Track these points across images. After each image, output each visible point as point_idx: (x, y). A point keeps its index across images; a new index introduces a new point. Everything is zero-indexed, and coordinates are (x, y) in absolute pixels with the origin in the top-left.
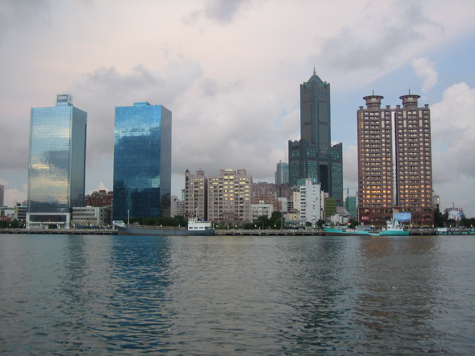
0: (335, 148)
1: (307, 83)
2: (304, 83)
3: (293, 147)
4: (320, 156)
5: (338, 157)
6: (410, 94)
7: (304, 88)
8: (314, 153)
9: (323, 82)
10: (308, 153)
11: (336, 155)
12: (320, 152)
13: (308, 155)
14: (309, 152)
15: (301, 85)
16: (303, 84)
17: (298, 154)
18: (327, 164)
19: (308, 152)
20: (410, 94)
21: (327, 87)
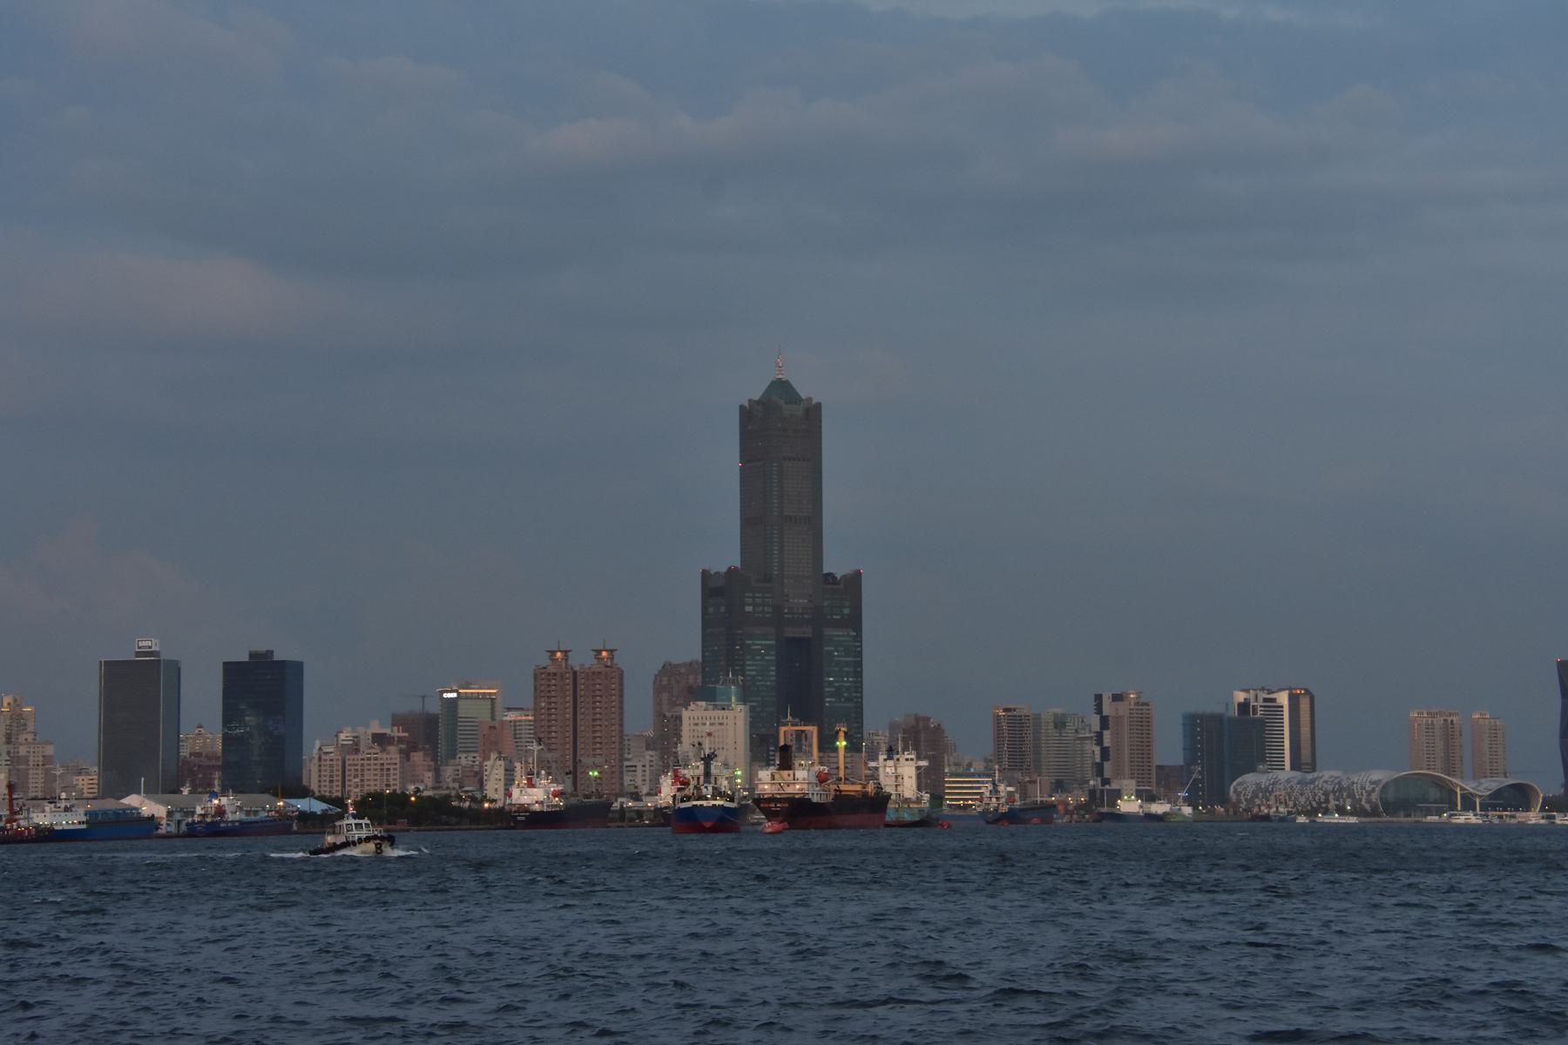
0: (835, 587)
1: (758, 402)
2: (750, 401)
3: (716, 590)
4: (787, 613)
5: (846, 611)
6: (604, 647)
7: (746, 414)
9: (804, 396)
10: (749, 609)
12: (787, 601)
13: (749, 612)
14: (754, 605)
15: (742, 407)
16: (746, 404)
17: (722, 609)
18: (810, 635)
19: (750, 605)
20: (604, 647)
21: (813, 413)
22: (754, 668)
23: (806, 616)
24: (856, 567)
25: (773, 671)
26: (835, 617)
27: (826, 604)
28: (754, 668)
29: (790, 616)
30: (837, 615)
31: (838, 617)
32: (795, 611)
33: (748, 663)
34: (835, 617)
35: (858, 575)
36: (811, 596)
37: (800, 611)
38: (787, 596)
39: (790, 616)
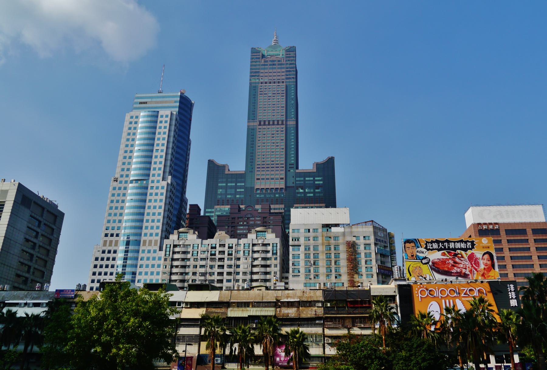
24: (330, 156)
29: (262, 196)
35: (330, 162)
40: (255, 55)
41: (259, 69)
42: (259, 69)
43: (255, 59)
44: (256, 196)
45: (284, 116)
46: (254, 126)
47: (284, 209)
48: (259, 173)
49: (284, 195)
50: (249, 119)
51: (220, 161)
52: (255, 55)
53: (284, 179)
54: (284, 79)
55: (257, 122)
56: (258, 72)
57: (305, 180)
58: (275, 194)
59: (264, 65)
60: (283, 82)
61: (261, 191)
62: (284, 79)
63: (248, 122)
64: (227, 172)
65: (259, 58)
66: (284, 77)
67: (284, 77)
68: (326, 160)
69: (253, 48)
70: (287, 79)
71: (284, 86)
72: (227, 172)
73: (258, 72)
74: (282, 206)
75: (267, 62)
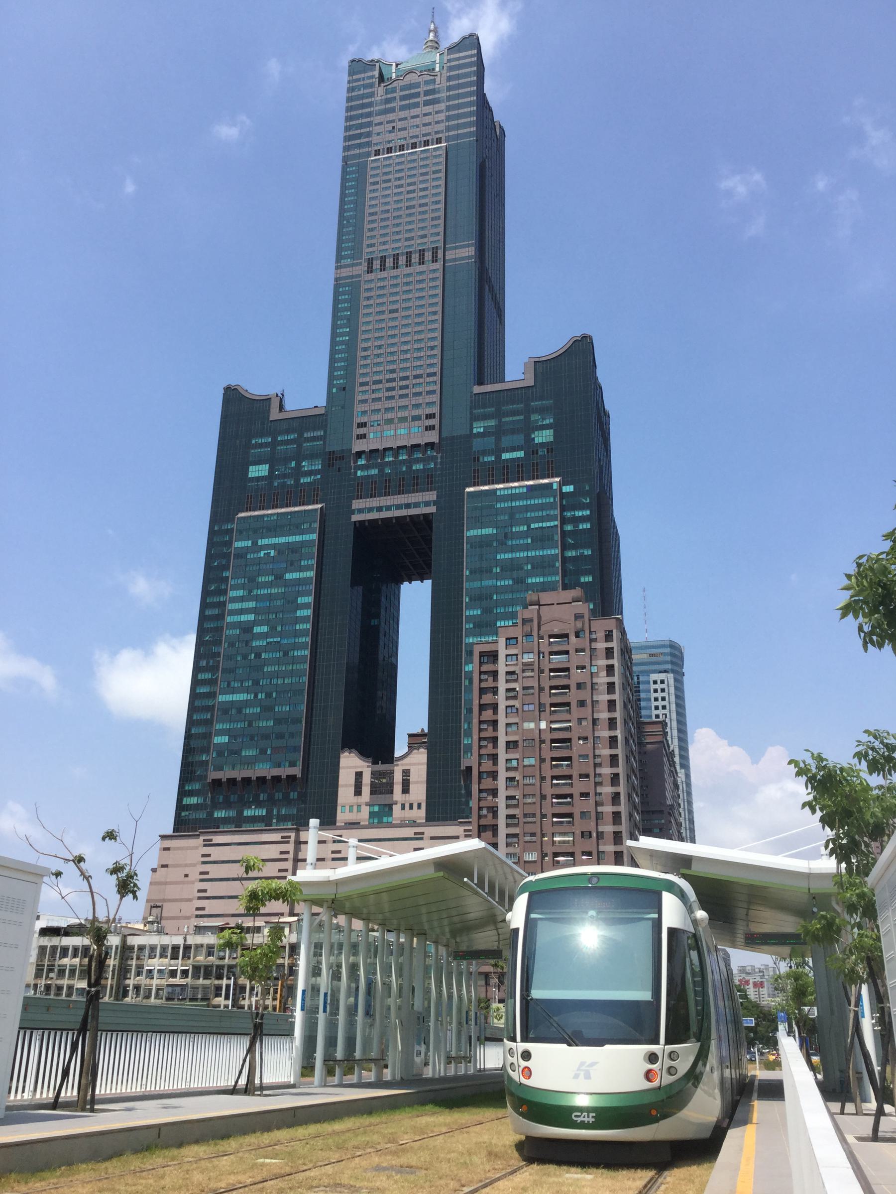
5: (543, 437)
8: (311, 457)
10: (258, 471)
11: (529, 428)
13: (258, 479)
14: (272, 461)
18: (432, 509)
22: (252, 604)
23: (420, 466)
25: (305, 606)
26: (505, 456)
27: (479, 428)
28: (252, 604)
29: (374, 472)
30: (513, 449)
31: (520, 454)
32: (390, 459)
33: (233, 594)
34: (505, 456)
36: (430, 416)
37: (403, 457)
38: (362, 425)
39: (374, 472)
40: (358, 80)
41: (369, 115)
42: (369, 115)
43: (359, 90)
44: (356, 473)
45: (441, 237)
46: (352, 277)
47: (435, 503)
48: (364, 407)
49: (435, 464)
50: (339, 257)
51: (256, 388)
52: (358, 80)
53: (437, 416)
54: (442, 132)
55: (361, 264)
56: (369, 124)
57: (498, 415)
58: (409, 463)
59: (388, 101)
60: (439, 141)
61: (368, 460)
62: (442, 132)
63: (337, 268)
64: (274, 415)
65: (371, 85)
66: (442, 127)
67: (442, 127)
68: (564, 349)
69: (353, 61)
70: (448, 129)
71: (443, 152)
72: (274, 415)
73: (369, 124)
74: (432, 496)
75: (394, 90)
